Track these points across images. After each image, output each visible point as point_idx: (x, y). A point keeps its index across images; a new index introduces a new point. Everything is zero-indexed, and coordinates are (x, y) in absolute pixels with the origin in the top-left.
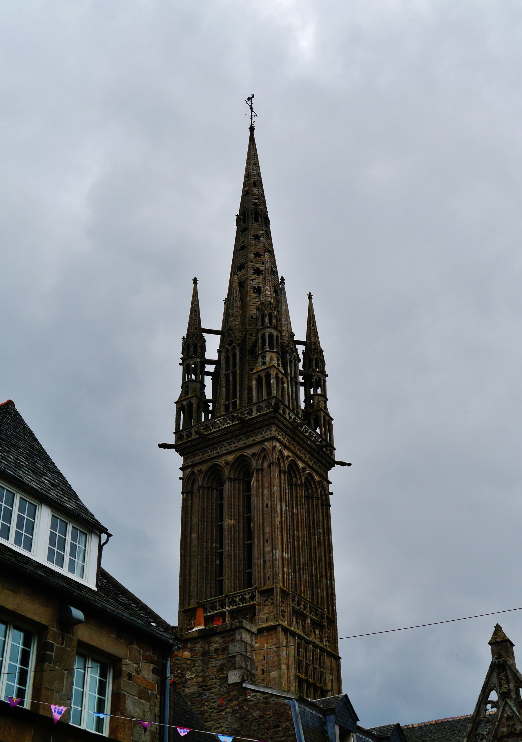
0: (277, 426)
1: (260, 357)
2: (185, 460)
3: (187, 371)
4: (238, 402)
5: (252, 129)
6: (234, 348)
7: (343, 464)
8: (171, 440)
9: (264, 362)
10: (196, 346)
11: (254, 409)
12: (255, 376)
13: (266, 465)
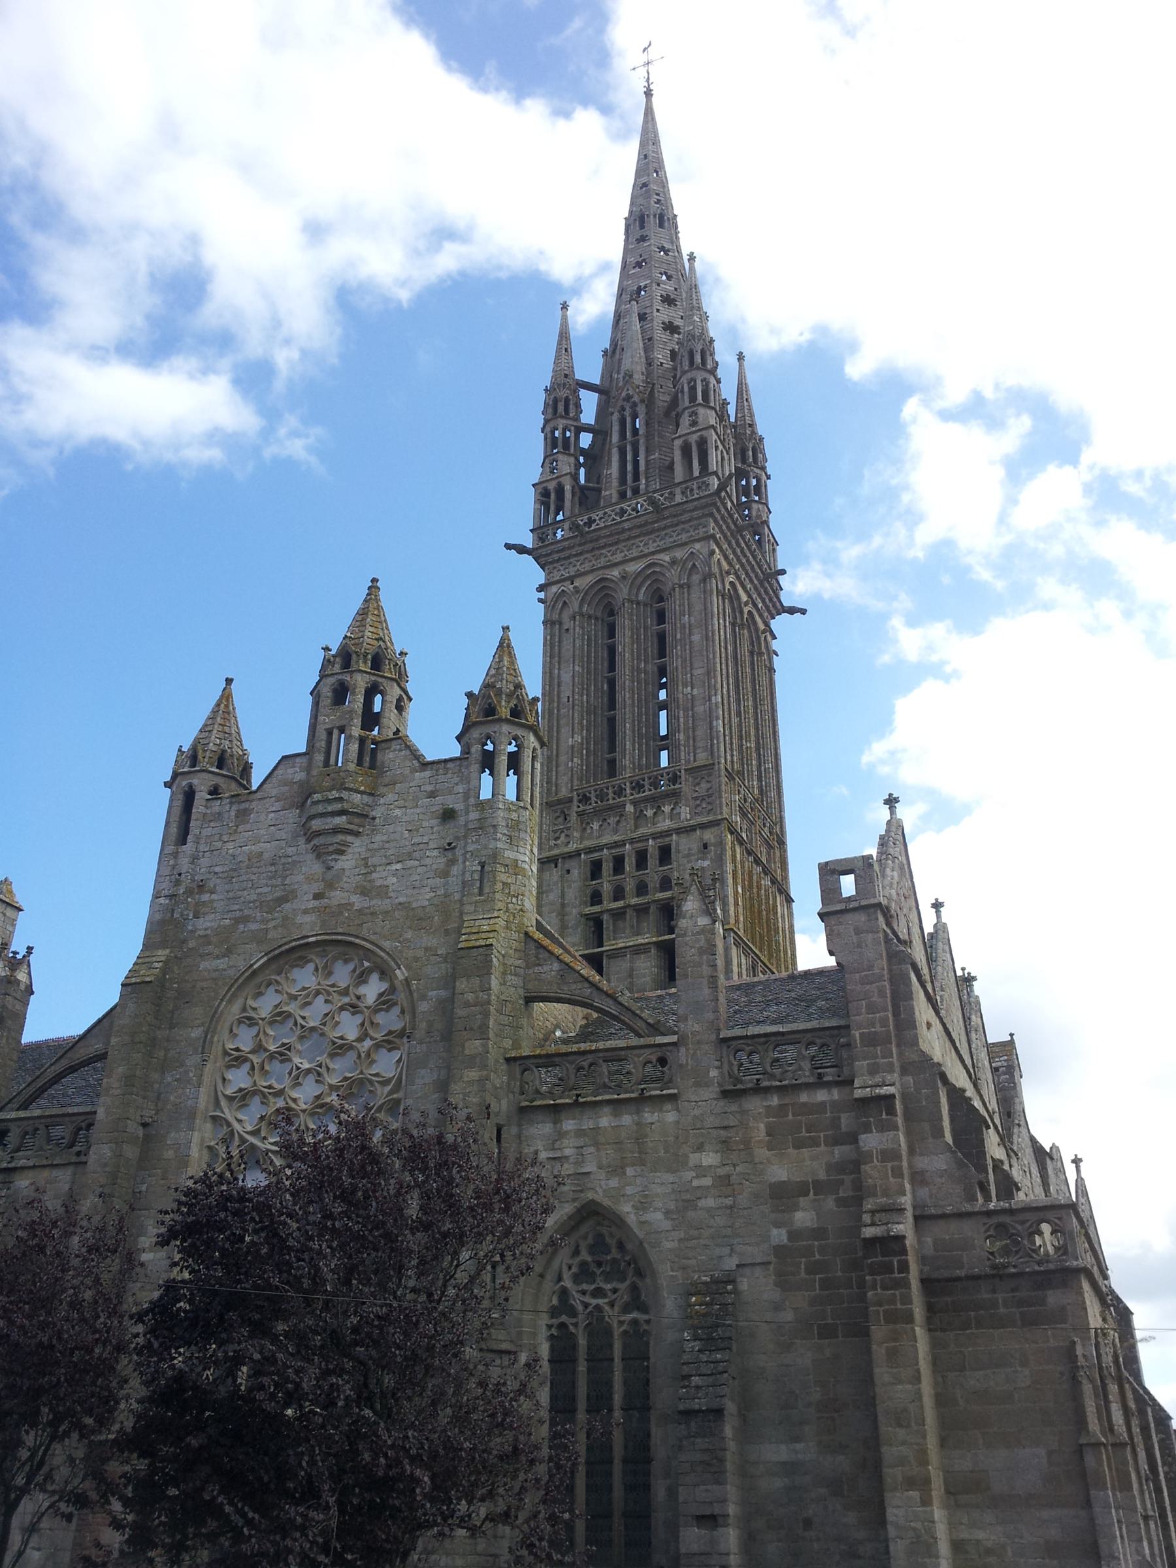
0: (716, 521)
1: (686, 413)
2: (547, 575)
3: (552, 443)
4: (642, 487)
5: (648, 94)
6: (635, 405)
7: (792, 611)
8: (528, 541)
9: (693, 421)
10: (567, 400)
11: (678, 491)
12: (678, 443)
13: (696, 578)
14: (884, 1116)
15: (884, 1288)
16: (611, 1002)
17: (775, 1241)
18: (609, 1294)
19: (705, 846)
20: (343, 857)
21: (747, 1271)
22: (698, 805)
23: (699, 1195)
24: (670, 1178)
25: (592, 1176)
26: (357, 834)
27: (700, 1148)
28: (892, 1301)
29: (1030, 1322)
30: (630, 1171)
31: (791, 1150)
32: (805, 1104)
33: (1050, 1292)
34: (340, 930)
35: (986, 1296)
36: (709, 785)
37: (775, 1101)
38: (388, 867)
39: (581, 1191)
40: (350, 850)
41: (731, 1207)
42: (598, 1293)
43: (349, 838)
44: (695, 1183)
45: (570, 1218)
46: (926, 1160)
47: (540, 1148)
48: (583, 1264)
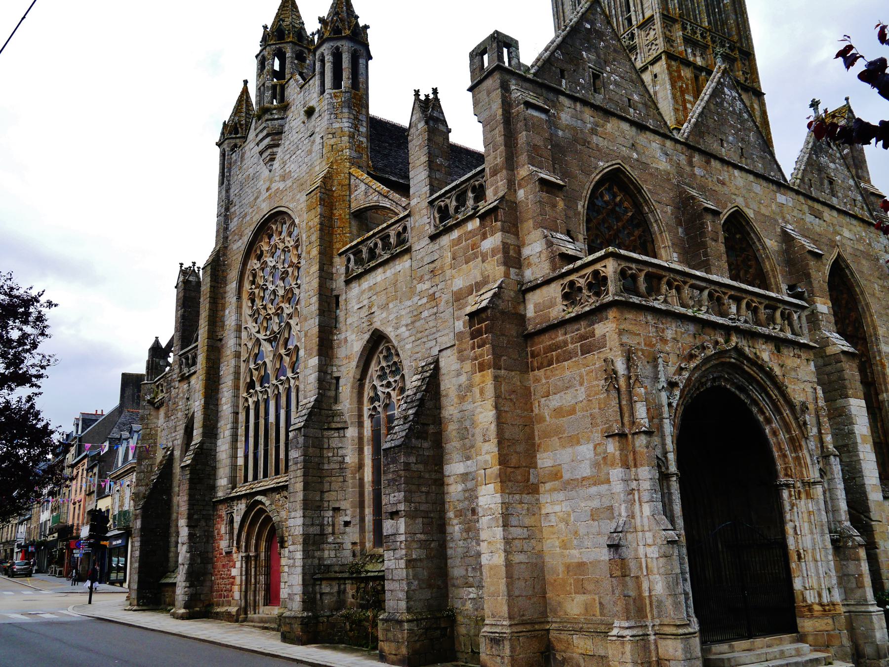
14: (494, 224)
15: (479, 347)
16: (387, 200)
17: (457, 330)
18: (393, 383)
19: (656, 76)
20: (275, 162)
21: (444, 353)
22: (650, 49)
23: (421, 310)
24: (409, 303)
25: (375, 314)
26: (278, 145)
27: (421, 280)
28: (481, 355)
29: (586, 350)
30: (391, 305)
31: (464, 266)
32: (470, 232)
33: (596, 326)
34: (276, 206)
35: (561, 338)
36: (654, 32)
37: (455, 234)
38: (291, 159)
39: (371, 324)
40: (277, 156)
41: (436, 314)
42: (389, 385)
43: (275, 150)
44: (420, 303)
45: (368, 342)
46: (530, 248)
47: (354, 304)
48: (382, 368)
